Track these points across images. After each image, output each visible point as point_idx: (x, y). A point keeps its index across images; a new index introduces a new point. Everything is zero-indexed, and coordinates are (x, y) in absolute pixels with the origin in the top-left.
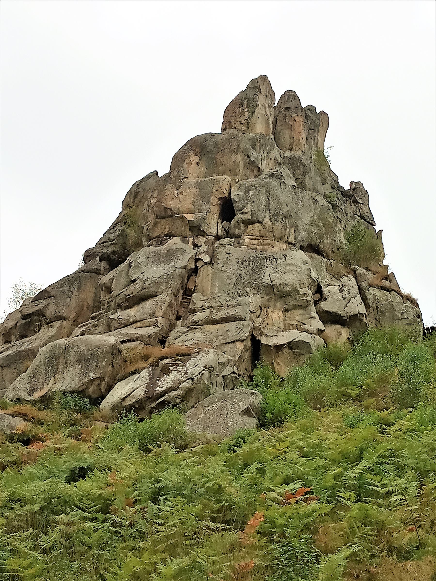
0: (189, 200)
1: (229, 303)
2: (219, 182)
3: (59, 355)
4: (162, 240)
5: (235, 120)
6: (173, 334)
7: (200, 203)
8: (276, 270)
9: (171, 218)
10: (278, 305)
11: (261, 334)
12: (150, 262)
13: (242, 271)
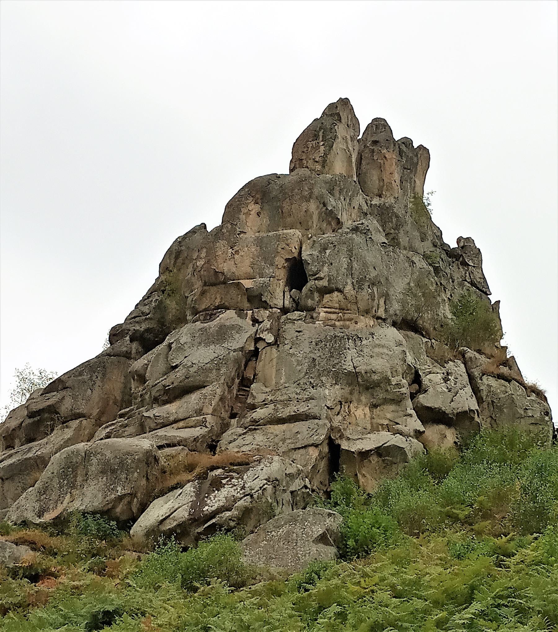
0: (247, 262)
2: (286, 238)
3: (78, 464)
4: (212, 314)
5: (307, 157)
6: (226, 437)
7: (261, 265)
8: (360, 353)
10: (363, 398)
11: (341, 437)
12: (196, 343)
13: (317, 355)
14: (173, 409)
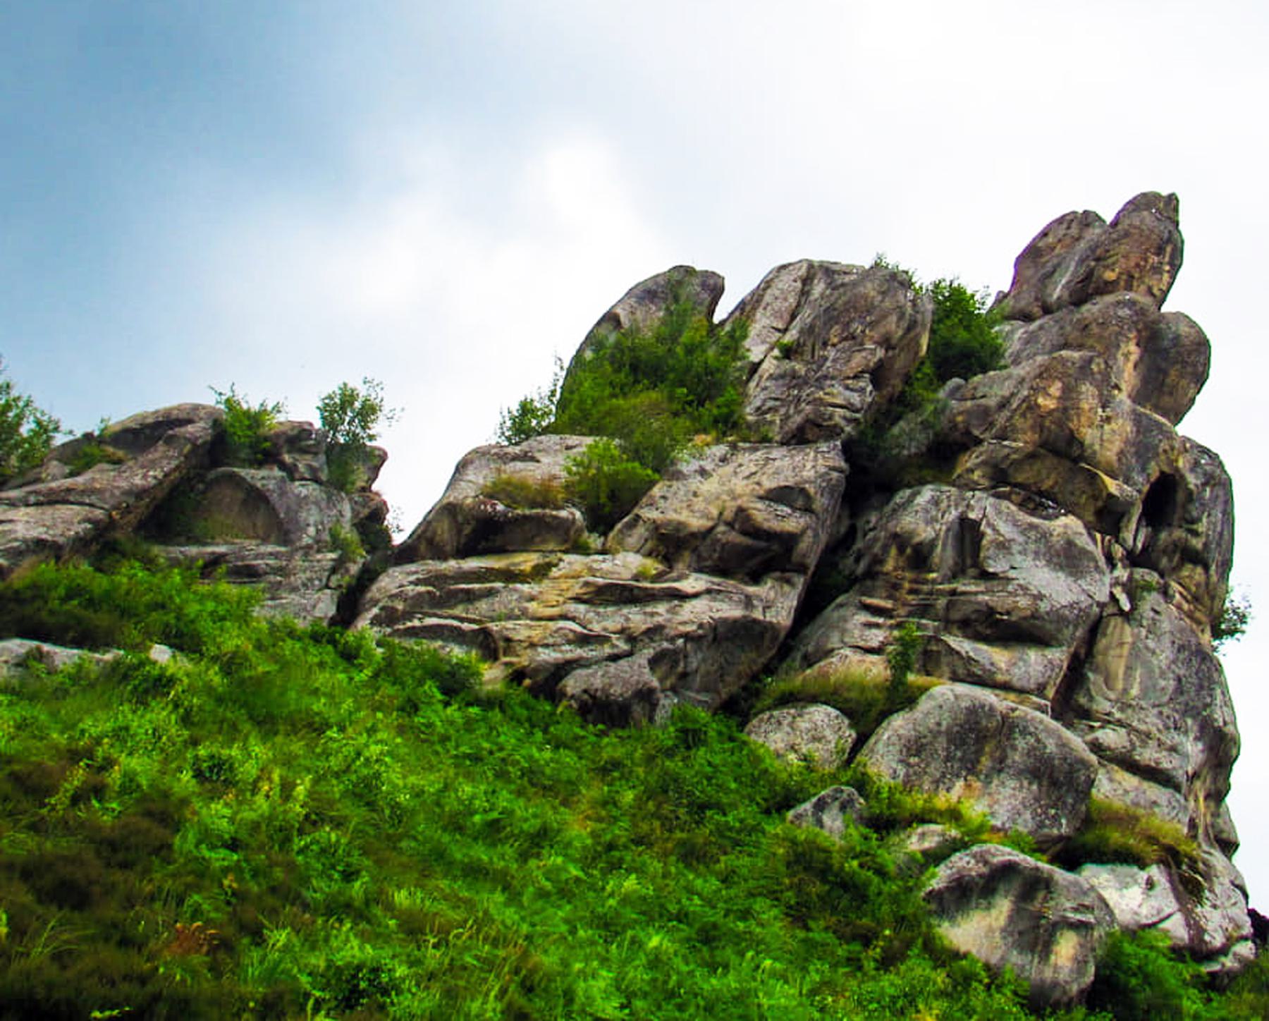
0: (1117, 446)
1: (1163, 738)
9: (1068, 464)
14: (997, 657)
